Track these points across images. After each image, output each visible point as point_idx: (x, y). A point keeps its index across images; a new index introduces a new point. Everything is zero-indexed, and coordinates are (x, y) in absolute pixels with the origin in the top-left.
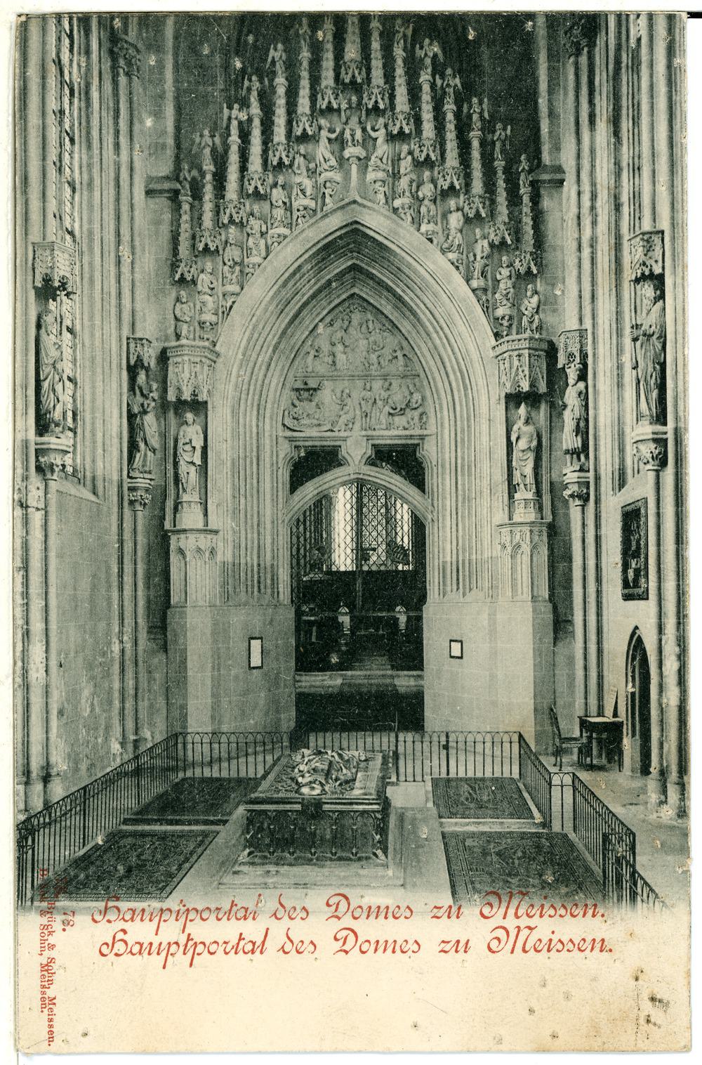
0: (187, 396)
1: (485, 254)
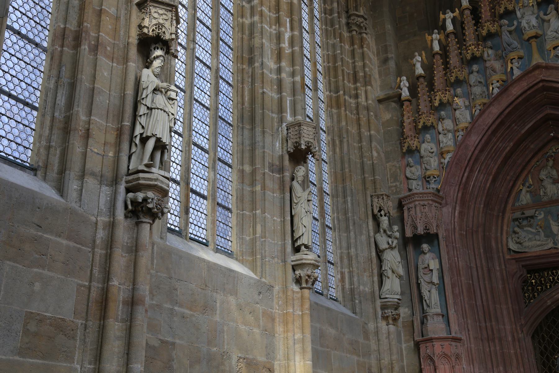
0: (421, 230)
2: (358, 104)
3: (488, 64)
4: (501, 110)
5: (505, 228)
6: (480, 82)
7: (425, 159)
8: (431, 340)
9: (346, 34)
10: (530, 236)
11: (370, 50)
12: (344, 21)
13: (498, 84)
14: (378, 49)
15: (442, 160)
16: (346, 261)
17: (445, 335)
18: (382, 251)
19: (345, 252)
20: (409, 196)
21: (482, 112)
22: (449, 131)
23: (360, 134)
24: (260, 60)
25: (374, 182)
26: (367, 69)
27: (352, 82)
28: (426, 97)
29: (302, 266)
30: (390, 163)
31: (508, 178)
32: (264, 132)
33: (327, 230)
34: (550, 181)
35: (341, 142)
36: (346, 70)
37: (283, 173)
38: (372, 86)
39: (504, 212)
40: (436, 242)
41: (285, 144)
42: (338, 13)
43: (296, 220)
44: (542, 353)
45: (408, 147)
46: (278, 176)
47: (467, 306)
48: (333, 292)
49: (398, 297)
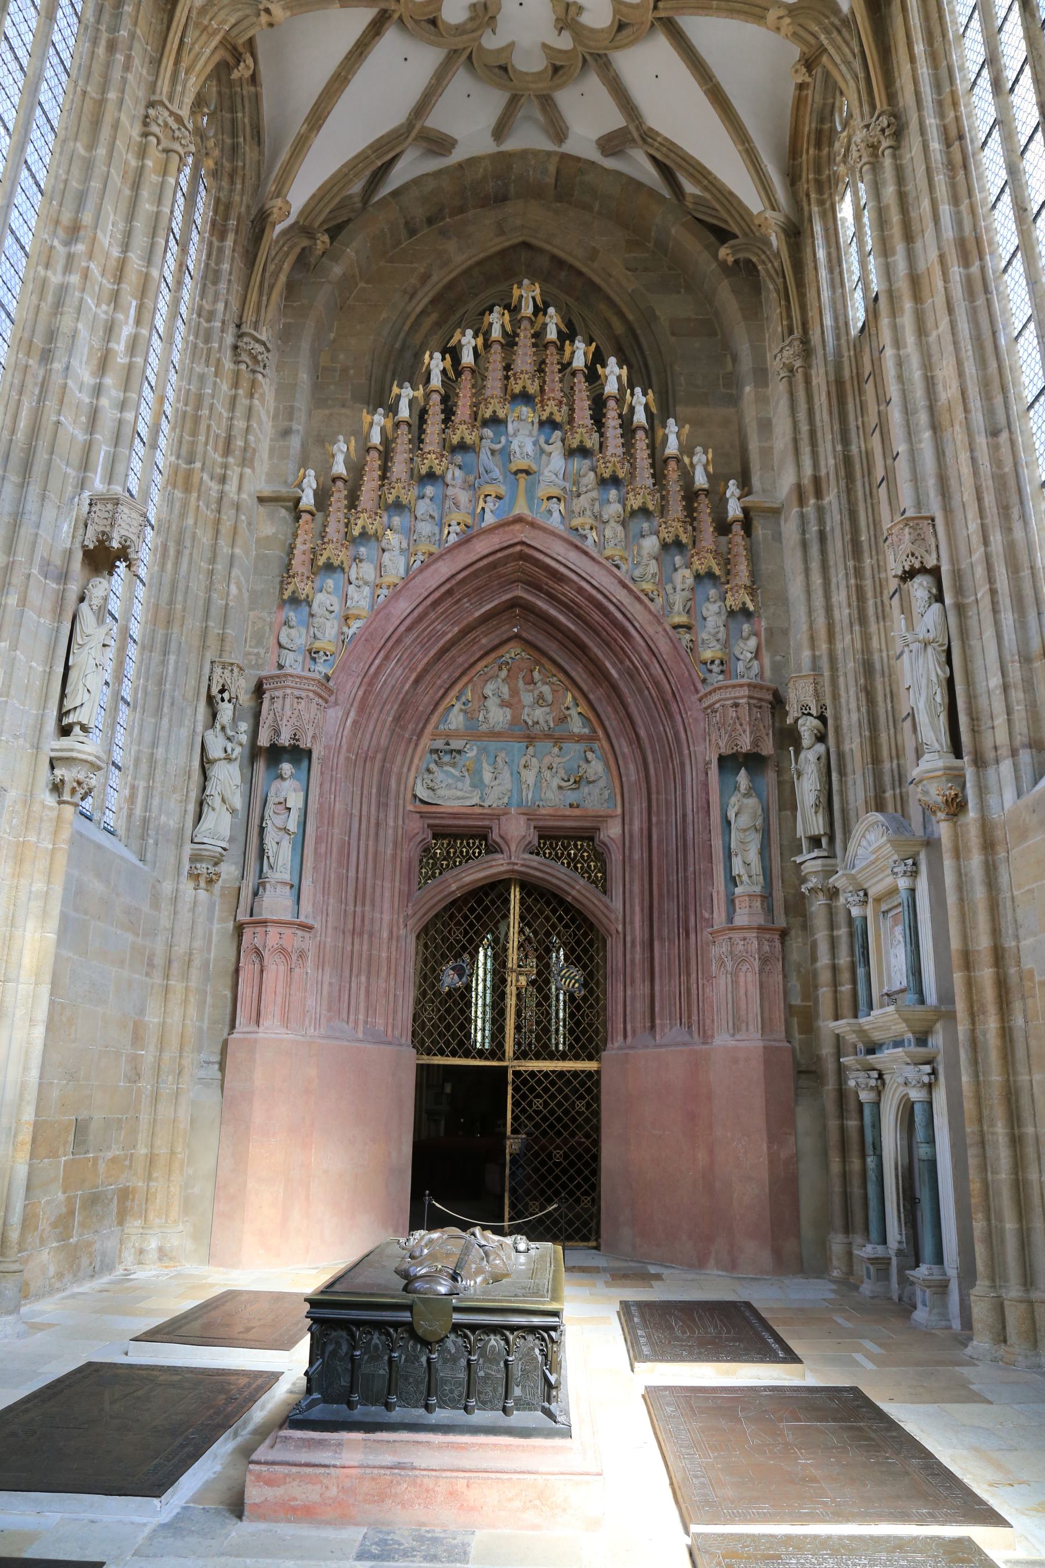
0: (285, 740)
1: (686, 586)
2: (222, 495)
3: (450, 491)
4: (454, 572)
5: (416, 761)
6: (431, 517)
7: (316, 620)
8: (264, 923)
9: (228, 365)
10: (450, 781)
11: (263, 405)
12: (229, 339)
13: (458, 529)
14: (277, 409)
15: (345, 629)
16: (144, 768)
17: (288, 918)
18: (211, 762)
19: (146, 750)
20: (278, 676)
21: (425, 566)
22: (366, 583)
23: (214, 548)
24: (65, 360)
25: (222, 639)
26: (251, 438)
27: (221, 451)
28: (341, 515)
29: (69, 761)
30: (256, 612)
31: (439, 682)
32: (43, 498)
33: (122, 706)
34: (498, 701)
35: (179, 553)
36: (214, 427)
37: (65, 584)
38: (253, 468)
39: (420, 736)
40: (305, 763)
41: (81, 531)
42: (223, 322)
43: (73, 675)
44: (425, 962)
45: (294, 592)
46: (54, 586)
47: (333, 876)
48: (110, 818)
49: (224, 845)
